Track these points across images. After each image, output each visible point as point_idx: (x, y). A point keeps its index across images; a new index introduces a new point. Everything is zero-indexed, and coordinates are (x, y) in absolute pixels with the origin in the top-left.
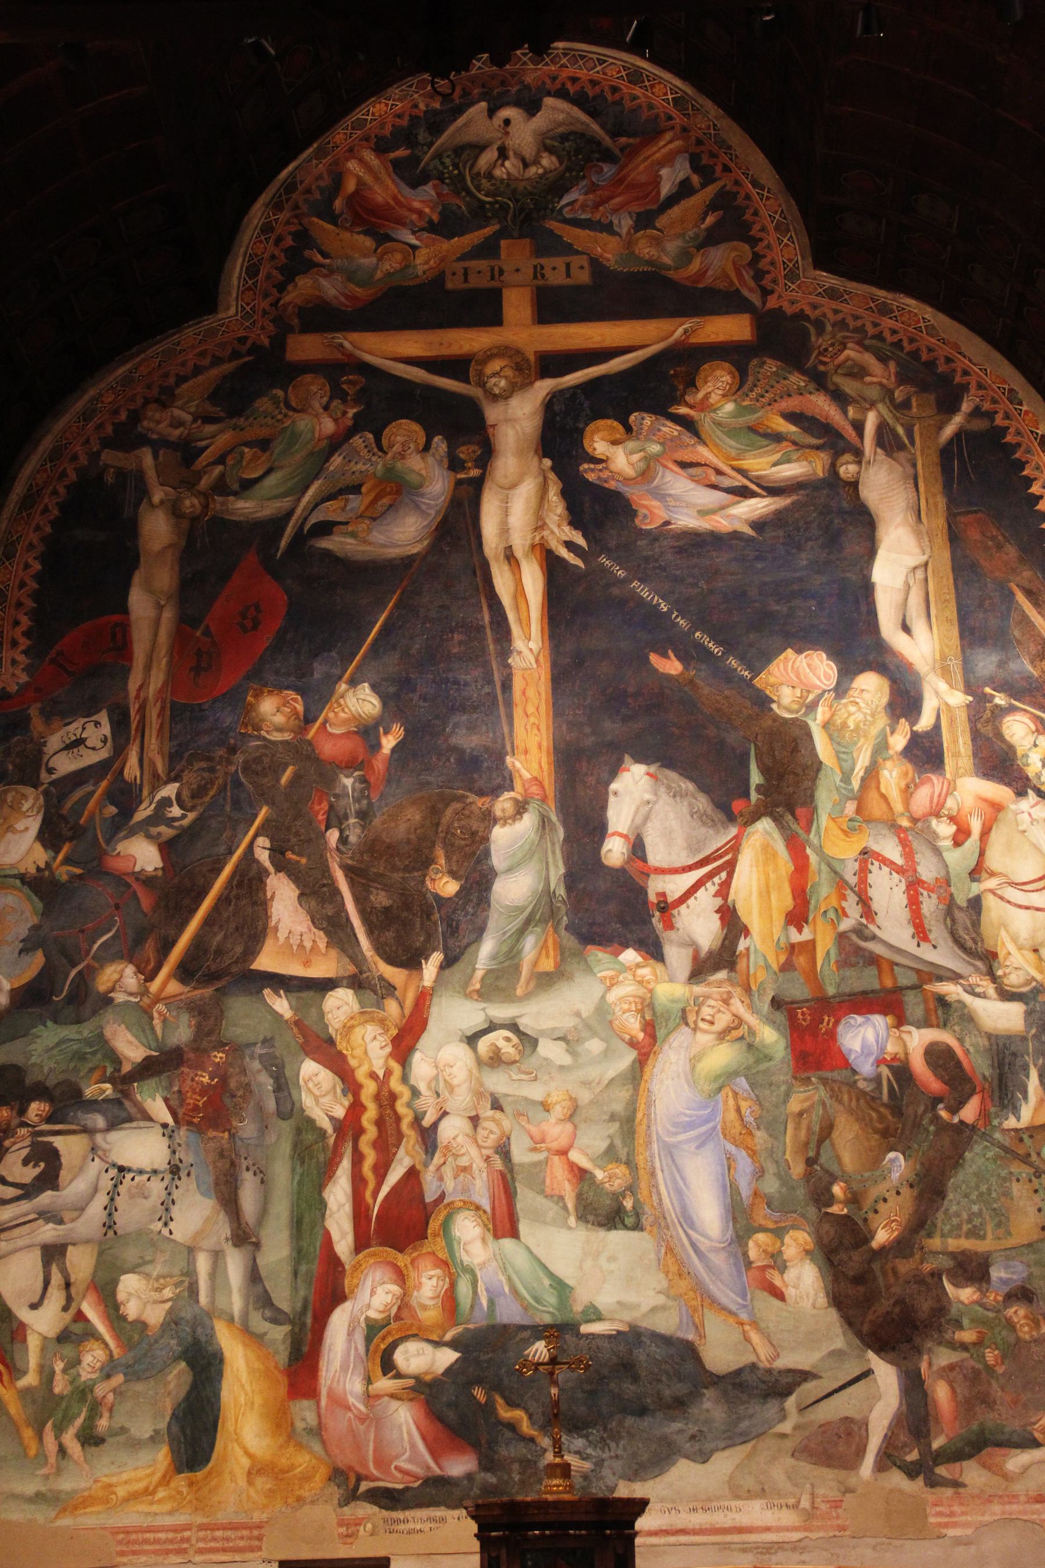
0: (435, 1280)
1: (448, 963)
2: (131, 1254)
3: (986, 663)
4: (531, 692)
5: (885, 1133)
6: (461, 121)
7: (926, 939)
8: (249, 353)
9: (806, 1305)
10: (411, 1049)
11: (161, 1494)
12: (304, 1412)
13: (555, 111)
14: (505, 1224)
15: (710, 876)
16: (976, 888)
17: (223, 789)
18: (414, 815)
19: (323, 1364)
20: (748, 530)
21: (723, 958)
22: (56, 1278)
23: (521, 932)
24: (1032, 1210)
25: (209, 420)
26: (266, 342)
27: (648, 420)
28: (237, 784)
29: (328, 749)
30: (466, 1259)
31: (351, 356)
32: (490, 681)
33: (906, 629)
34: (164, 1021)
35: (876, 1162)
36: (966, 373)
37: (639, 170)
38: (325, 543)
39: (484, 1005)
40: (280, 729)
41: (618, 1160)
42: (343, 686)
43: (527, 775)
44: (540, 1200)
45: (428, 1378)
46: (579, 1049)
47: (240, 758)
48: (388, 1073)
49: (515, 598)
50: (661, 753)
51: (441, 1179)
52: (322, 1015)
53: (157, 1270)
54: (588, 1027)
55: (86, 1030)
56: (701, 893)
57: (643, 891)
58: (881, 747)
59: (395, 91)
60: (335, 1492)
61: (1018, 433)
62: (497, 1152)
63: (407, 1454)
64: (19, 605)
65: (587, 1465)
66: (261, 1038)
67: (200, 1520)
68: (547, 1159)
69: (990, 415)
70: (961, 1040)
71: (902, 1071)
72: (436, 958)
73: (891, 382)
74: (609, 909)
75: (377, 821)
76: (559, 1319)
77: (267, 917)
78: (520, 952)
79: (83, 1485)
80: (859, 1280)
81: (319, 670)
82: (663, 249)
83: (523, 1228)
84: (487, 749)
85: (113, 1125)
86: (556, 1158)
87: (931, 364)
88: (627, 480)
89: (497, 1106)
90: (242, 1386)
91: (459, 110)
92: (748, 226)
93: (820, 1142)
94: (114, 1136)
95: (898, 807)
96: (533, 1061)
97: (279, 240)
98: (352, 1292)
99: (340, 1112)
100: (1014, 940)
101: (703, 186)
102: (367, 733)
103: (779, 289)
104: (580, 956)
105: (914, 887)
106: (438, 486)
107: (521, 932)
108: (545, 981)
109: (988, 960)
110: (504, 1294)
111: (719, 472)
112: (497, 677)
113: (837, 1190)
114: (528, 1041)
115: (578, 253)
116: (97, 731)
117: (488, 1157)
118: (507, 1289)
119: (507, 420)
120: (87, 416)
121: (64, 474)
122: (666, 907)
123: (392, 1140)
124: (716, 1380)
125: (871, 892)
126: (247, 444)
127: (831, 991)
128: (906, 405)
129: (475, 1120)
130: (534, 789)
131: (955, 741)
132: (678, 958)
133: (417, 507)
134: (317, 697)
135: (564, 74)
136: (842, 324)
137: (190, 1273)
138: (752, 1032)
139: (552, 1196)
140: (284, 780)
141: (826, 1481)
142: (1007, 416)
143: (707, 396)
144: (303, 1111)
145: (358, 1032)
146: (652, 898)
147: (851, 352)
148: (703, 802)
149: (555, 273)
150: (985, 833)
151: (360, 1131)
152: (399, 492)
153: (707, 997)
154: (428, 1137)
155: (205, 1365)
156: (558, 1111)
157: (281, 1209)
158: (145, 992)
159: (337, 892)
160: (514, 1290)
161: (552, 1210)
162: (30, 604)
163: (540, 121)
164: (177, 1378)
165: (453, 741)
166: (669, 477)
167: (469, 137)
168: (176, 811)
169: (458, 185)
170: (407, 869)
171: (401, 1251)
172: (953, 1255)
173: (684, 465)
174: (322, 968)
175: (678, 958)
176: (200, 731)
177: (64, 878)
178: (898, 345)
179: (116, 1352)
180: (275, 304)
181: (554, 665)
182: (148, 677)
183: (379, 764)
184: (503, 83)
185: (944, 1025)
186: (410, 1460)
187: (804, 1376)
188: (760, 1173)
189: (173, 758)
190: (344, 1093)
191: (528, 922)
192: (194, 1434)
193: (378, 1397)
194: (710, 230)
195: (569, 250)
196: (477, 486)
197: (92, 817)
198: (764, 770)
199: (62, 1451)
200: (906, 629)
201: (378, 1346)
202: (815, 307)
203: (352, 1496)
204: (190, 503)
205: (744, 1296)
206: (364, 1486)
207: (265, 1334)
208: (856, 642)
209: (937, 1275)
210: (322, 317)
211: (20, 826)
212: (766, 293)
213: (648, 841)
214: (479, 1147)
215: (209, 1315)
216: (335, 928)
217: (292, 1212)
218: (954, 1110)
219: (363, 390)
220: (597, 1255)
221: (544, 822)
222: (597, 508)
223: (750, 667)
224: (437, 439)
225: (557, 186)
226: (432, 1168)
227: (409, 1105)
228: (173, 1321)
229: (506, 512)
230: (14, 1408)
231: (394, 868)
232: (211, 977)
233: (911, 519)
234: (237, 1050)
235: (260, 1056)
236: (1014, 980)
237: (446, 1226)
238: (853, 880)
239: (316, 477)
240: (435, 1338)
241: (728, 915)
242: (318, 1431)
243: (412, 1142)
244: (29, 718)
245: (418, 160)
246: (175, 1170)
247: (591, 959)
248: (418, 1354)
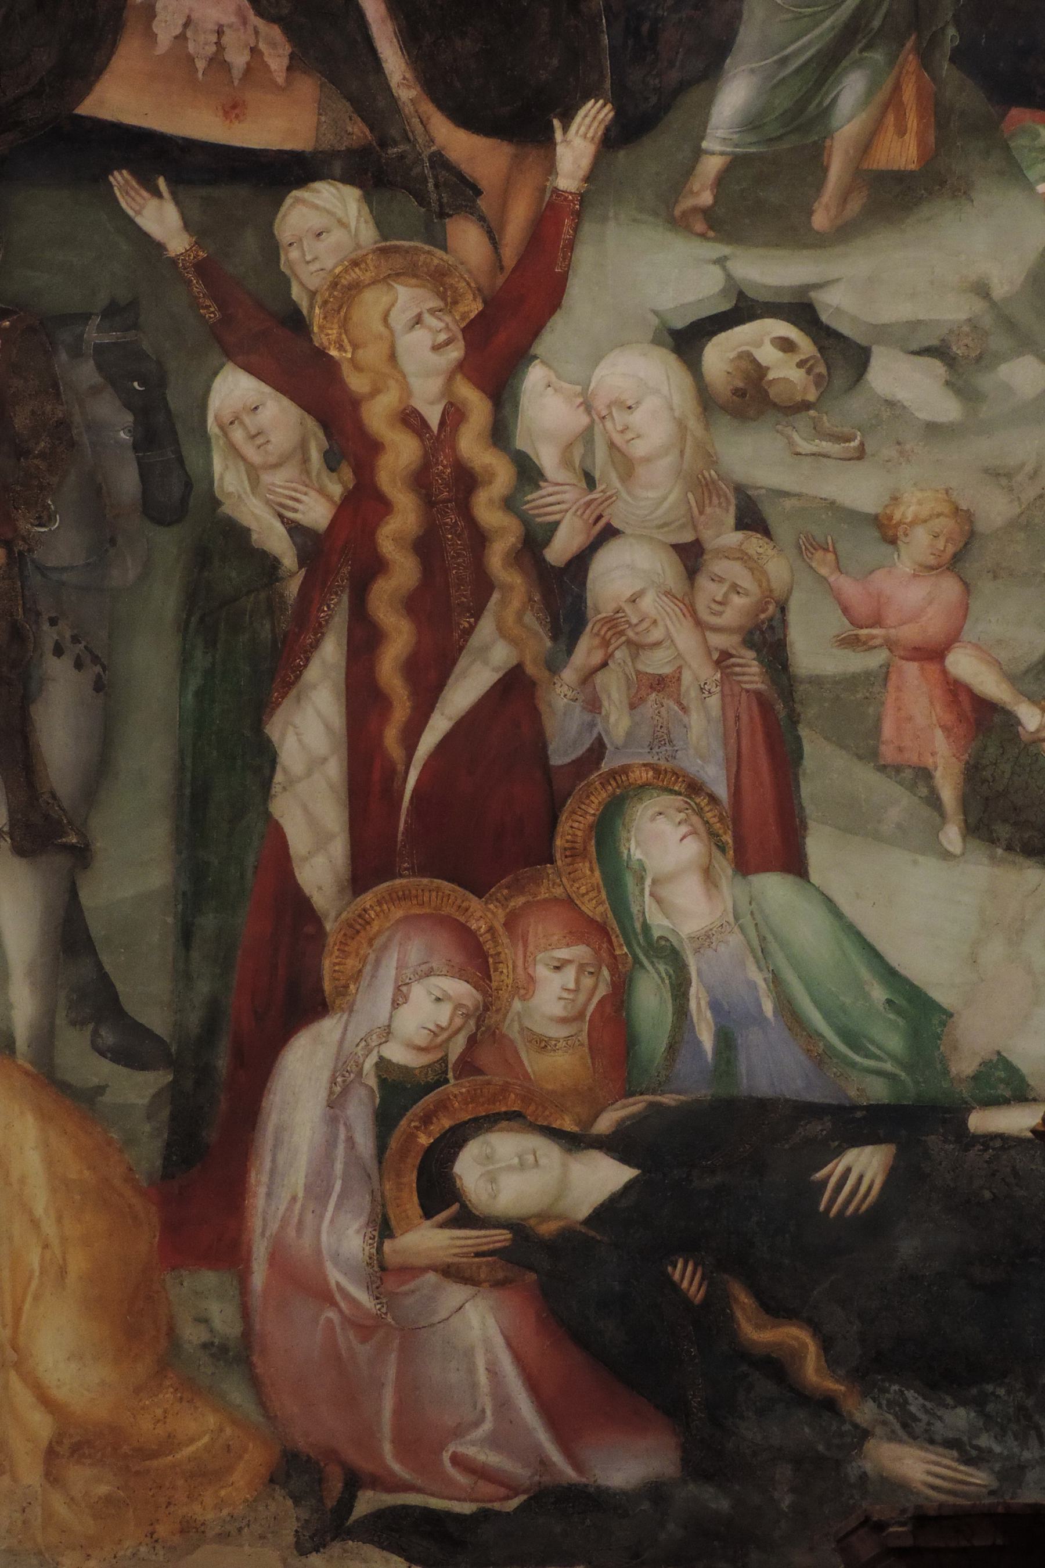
0: (570, 972)
10: (519, 357)
12: (205, 1306)
14: (765, 833)
19: (259, 1180)
23: (828, 64)
39: (725, 250)
44: (866, 776)
45: (547, 1229)
46: (985, 382)
48: (454, 415)
51: (594, 705)
52: (272, 249)
54: (1010, 325)
60: (288, 1515)
62: (749, 642)
63: (487, 1426)
66: (102, 300)
68: (887, 667)
72: (593, 117)
78: (826, 113)
83: (818, 847)
86: (912, 669)
89: (751, 517)
90: (35, 1223)
96: (856, 405)
98: (342, 991)
104: (989, 134)
108: (894, 197)
110: (759, 1019)
114: (842, 355)
117: (725, 655)
118: (768, 1007)
129: (691, 556)
139: (898, 769)
144: (217, 503)
145: (371, 304)
154: (563, 596)
156: (920, 544)
157: (150, 760)
160: (788, 1011)
161: (899, 804)
171: (479, 892)
174: (279, 122)
186: (493, 1441)
190: (331, 463)
193: (409, 1271)
201: (411, 1137)
203: (331, 1527)
206: (366, 1502)
207: (101, 1090)
214: (700, 624)
217: (181, 768)
226: (569, 675)
227: (509, 504)
235: (100, 350)
237: (606, 832)
240: (568, 1124)
242: (239, 1355)
243: (516, 604)
247: (1018, 143)
248: (522, 1166)
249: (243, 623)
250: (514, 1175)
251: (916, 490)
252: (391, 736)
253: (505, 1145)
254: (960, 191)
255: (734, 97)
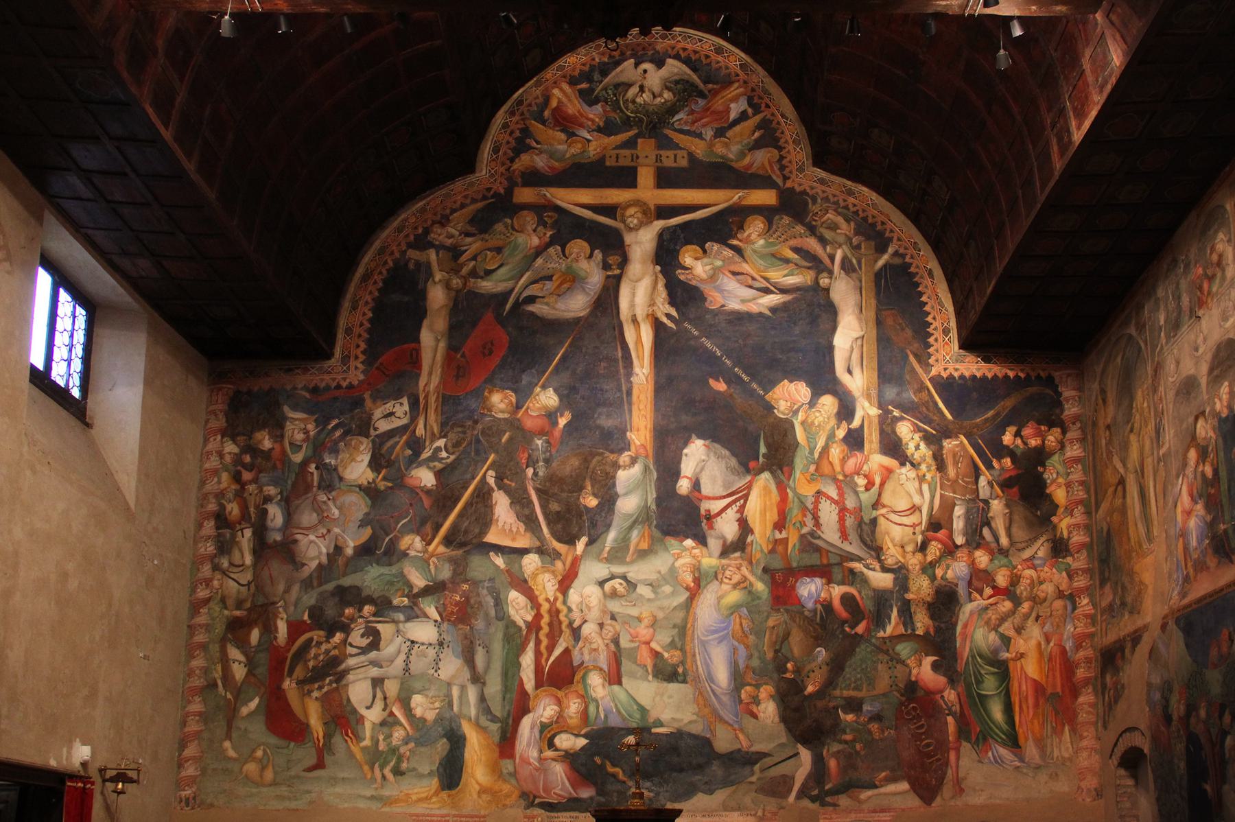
1: (591, 542)
2: (418, 685)
3: (891, 392)
4: (642, 397)
5: (816, 638)
6: (619, 69)
7: (846, 539)
8: (492, 197)
9: (769, 721)
10: (568, 587)
11: (434, 799)
12: (507, 766)
13: (673, 67)
14: (614, 677)
15: (734, 502)
16: (875, 513)
17: (470, 444)
18: (576, 462)
19: (517, 743)
20: (768, 313)
21: (738, 546)
22: (379, 695)
23: (631, 528)
24: (887, 677)
25: (468, 235)
26: (502, 191)
27: (716, 247)
28: (478, 441)
29: (529, 424)
30: (594, 695)
31: (549, 201)
32: (620, 390)
33: (850, 372)
34: (436, 567)
35: (810, 652)
36: (892, 231)
37: (718, 104)
38: (530, 308)
40: (503, 412)
41: (676, 648)
42: (538, 389)
43: (638, 443)
44: (634, 666)
47: (480, 426)
48: (556, 599)
49: (636, 343)
50: (712, 434)
52: (521, 567)
53: (431, 693)
54: (665, 579)
55: (394, 570)
56: (729, 510)
57: (698, 508)
58: (831, 436)
59: (582, 50)
61: (917, 267)
64: (360, 336)
65: (652, 795)
67: (454, 812)
69: (903, 256)
70: (860, 592)
71: (828, 606)
72: (584, 540)
73: (851, 234)
74: (679, 517)
75: (554, 465)
76: (641, 725)
77: (493, 514)
79: (395, 793)
80: (797, 710)
81: (525, 379)
82: (731, 149)
83: (624, 680)
84: (616, 428)
85: (408, 620)
87: (873, 225)
88: (702, 280)
89: (613, 618)
91: (618, 63)
92: (777, 140)
93: (782, 642)
94: (409, 625)
95: (838, 469)
96: (634, 595)
97: (512, 133)
99: (529, 618)
100: (892, 540)
101: (754, 115)
102: (551, 416)
103: (793, 176)
104: (662, 541)
105: (843, 511)
106: (595, 278)
107: (631, 528)
108: (643, 554)
109: (877, 551)
111: (753, 279)
112: (624, 388)
113: (789, 665)
114: (632, 585)
115: (681, 149)
116: (401, 408)
119: (636, 243)
120: (399, 230)
121: (386, 263)
122: (710, 518)
123: (557, 634)
124: (719, 756)
125: (820, 514)
126: (489, 249)
127: (795, 565)
128: (858, 247)
129: (601, 625)
130: (642, 451)
131: (871, 434)
132: (714, 544)
133: (584, 289)
134: (523, 395)
135: (680, 46)
136: (826, 199)
137: (449, 696)
138: (751, 585)
140: (504, 440)
141: (771, 804)
142: (912, 257)
143: (749, 236)
145: (540, 577)
146: (703, 512)
147: (830, 216)
148: (733, 462)
149: (668, 159)
150: (882, 484)
151: (539, 628)
152: (574, 281)
153: (729, 566)
154: (576, 633)
155: (456, 741)
157: (497, 666)
158: (426, 551)
159: (531, 502)
160: (618, 711)
161: (640, 672)
162: (366, 335)
163: (664, 72)
164: (442, 746)
165: (598, 422)
166: (726, 280)
167: (623, 79)
168: (444, 454)
169: (616, 107)
170: (571, 492)
172: (845, 699)
173: (735, 274)
174: (521, 543)
175: (714, 544)
176: (457, 410)
177: (382, 488)
178: (856, 213)
179: (411, 732)
180: (507, 170)
181: (656, 383)
182: (430, 379)
183: (557, 433)
184: (644, 49)
185: (852, 584)
187: (765, 755)
188: (750, 657)
189: (443, 425)
191: (635, 522)
192: (451, 773)
193: (546, 759)
194: (756, 140)
195: (677, 147)
196: (618, 278)
197: (398, 455)
198: (768, 446)
199: (384, 777)
200: (850, 372)
202: (812, 188)
203: (531, 805)
204: (456, 282)
205: (737, 716)
206: (537, 801)
208: (822, 378)
209: (836, 708)
210: (534, 178)
211: (359, 459)
212: (785, 178)
213: (702, 482)
215: (459, 716)
216: (530, 522)
218: (852, 627)
219: (556, 222)
220: (662, 695)
221: (646, 468)
222: (684, 295)
223: (764, 390)
224: (596, 251)
225: (672, 110)
227: (566, 616)
228: (439, 719)
229: (634, 295)
230: (359, 756)
231: (563, 491)
232: (462, 545)
233: (857, 310)
234: (475, 583)
236: (890, 561)
237: (584, 678)
238: (810, 507)
239: (528, 270)
241: (743, 524)
242: (514, 774)
244: (364, 400)
245: (593, 90)
246: (441, 644)
249: (515, 640)
250: (566, 742)
251: (645, 611)
252: (543, 661)
253: (564, 736)
254: (656, 553)
255: (612, 535)
